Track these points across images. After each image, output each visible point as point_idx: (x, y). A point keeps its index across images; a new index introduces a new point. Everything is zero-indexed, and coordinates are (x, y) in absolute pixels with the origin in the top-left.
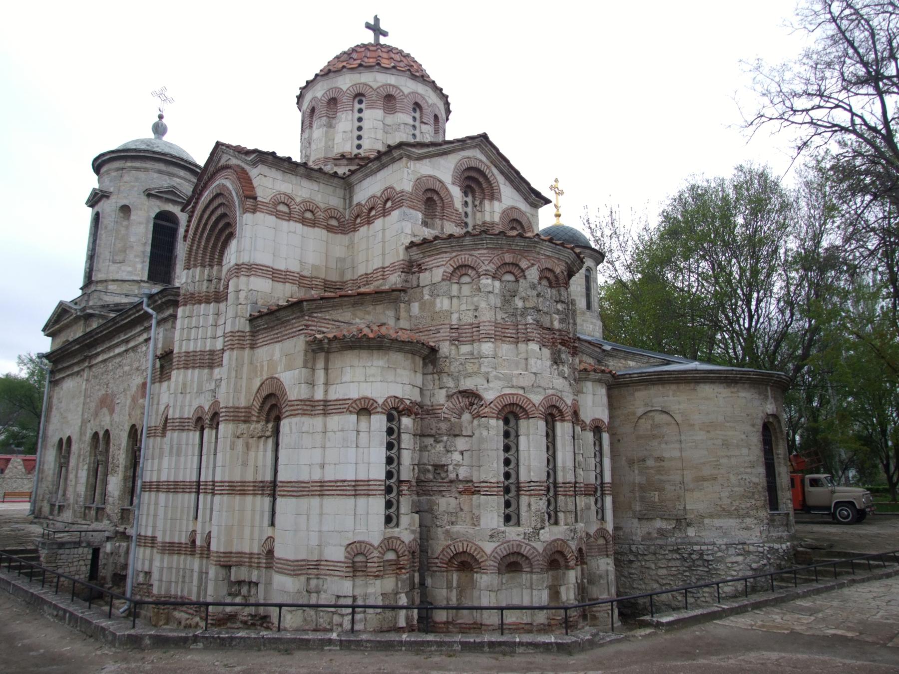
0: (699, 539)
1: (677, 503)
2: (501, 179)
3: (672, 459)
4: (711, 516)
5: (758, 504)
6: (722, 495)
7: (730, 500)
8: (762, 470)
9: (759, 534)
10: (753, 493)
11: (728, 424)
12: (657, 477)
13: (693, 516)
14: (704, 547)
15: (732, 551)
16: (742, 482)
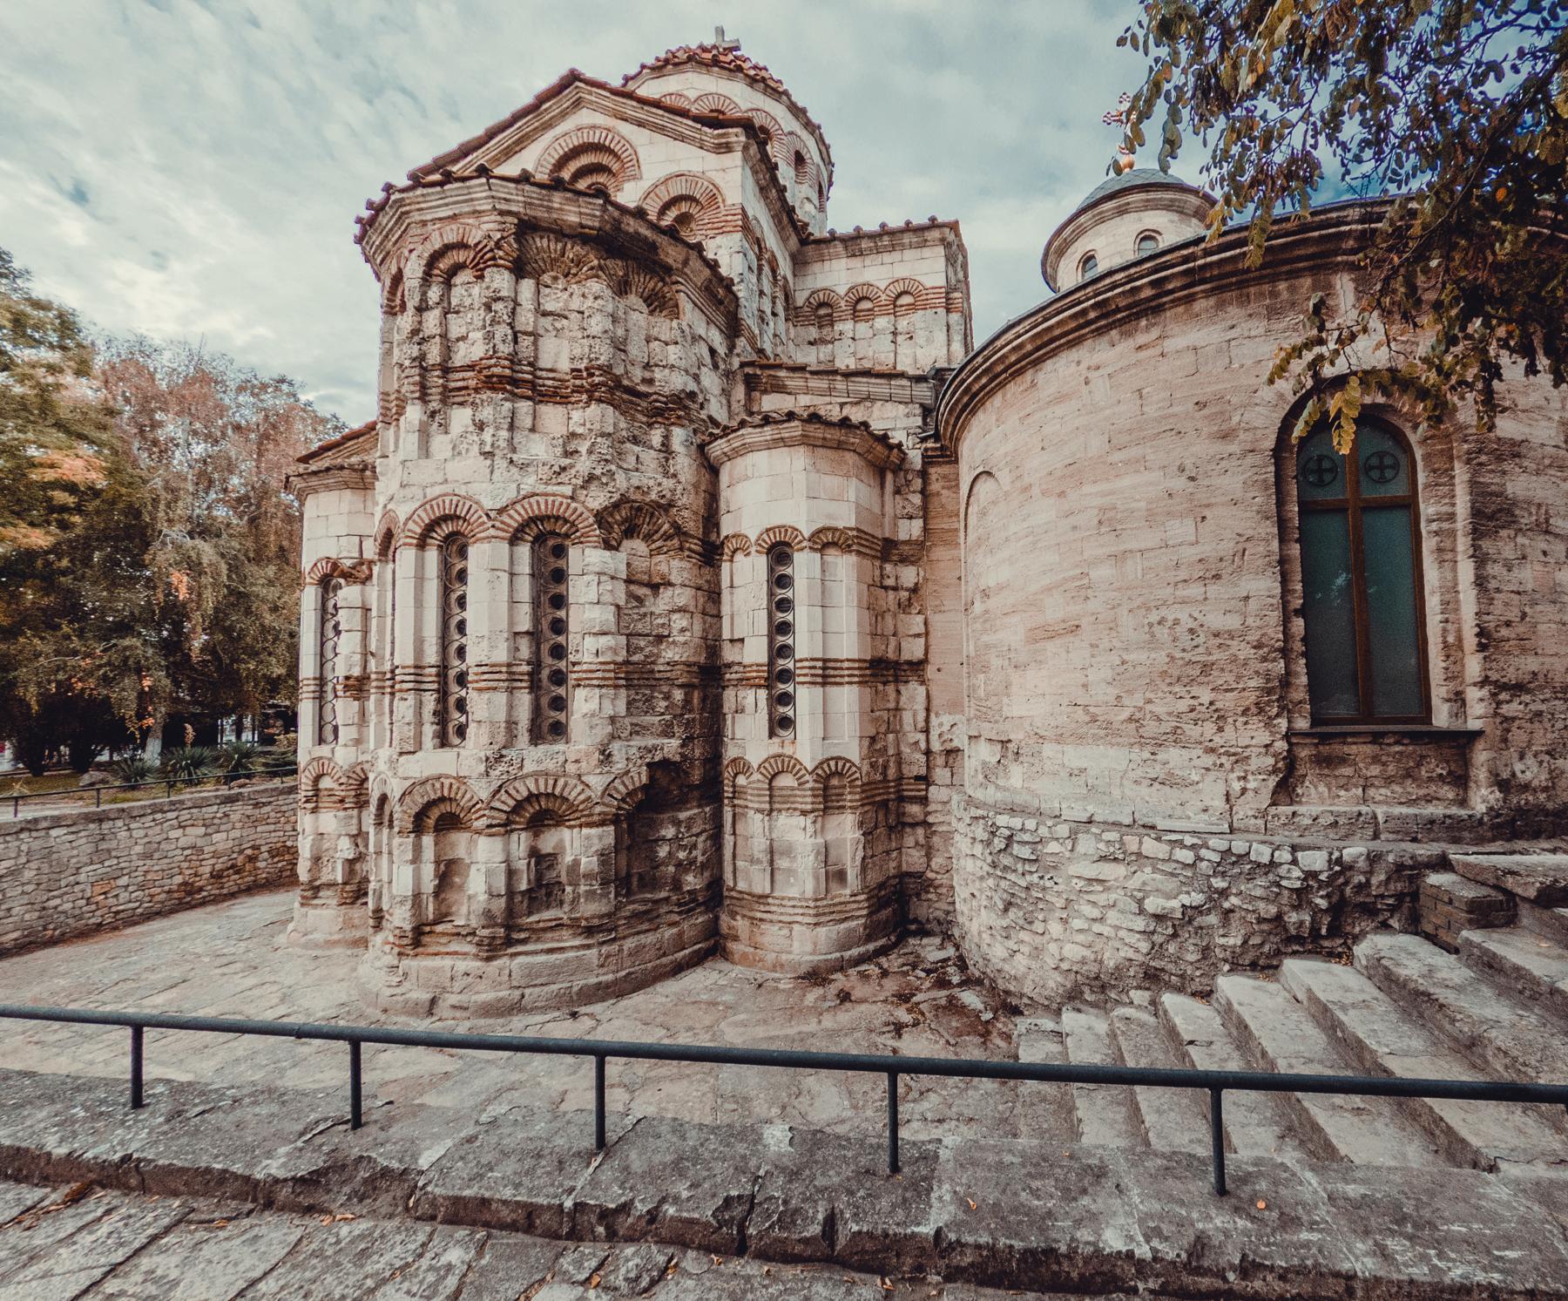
0: (1028, 798)
1: (1005, 700)
2: (626, 129)
3: (1001, 588)
4: (1059, 739)
5: (1227, 701)
6: (1093, 676)
7: (1114, 691)
8: (1265, 586)
9: (1220, 804)
10: (1206, 668)
11: (1117, 456)
12: (985, 638)
13: (1021, 736)
14: (1016, 822)
15: (1086, 844)
16: (1163, 633)
